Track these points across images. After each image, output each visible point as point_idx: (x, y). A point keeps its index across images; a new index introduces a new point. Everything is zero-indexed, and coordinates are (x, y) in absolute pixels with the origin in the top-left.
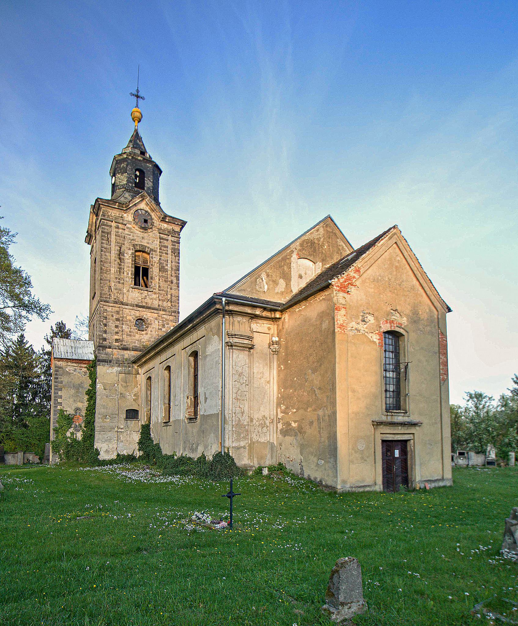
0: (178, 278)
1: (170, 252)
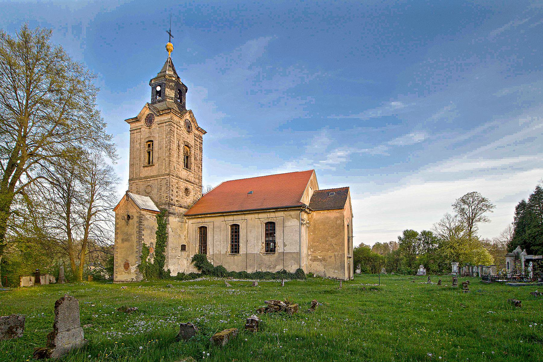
0: (201, 165)
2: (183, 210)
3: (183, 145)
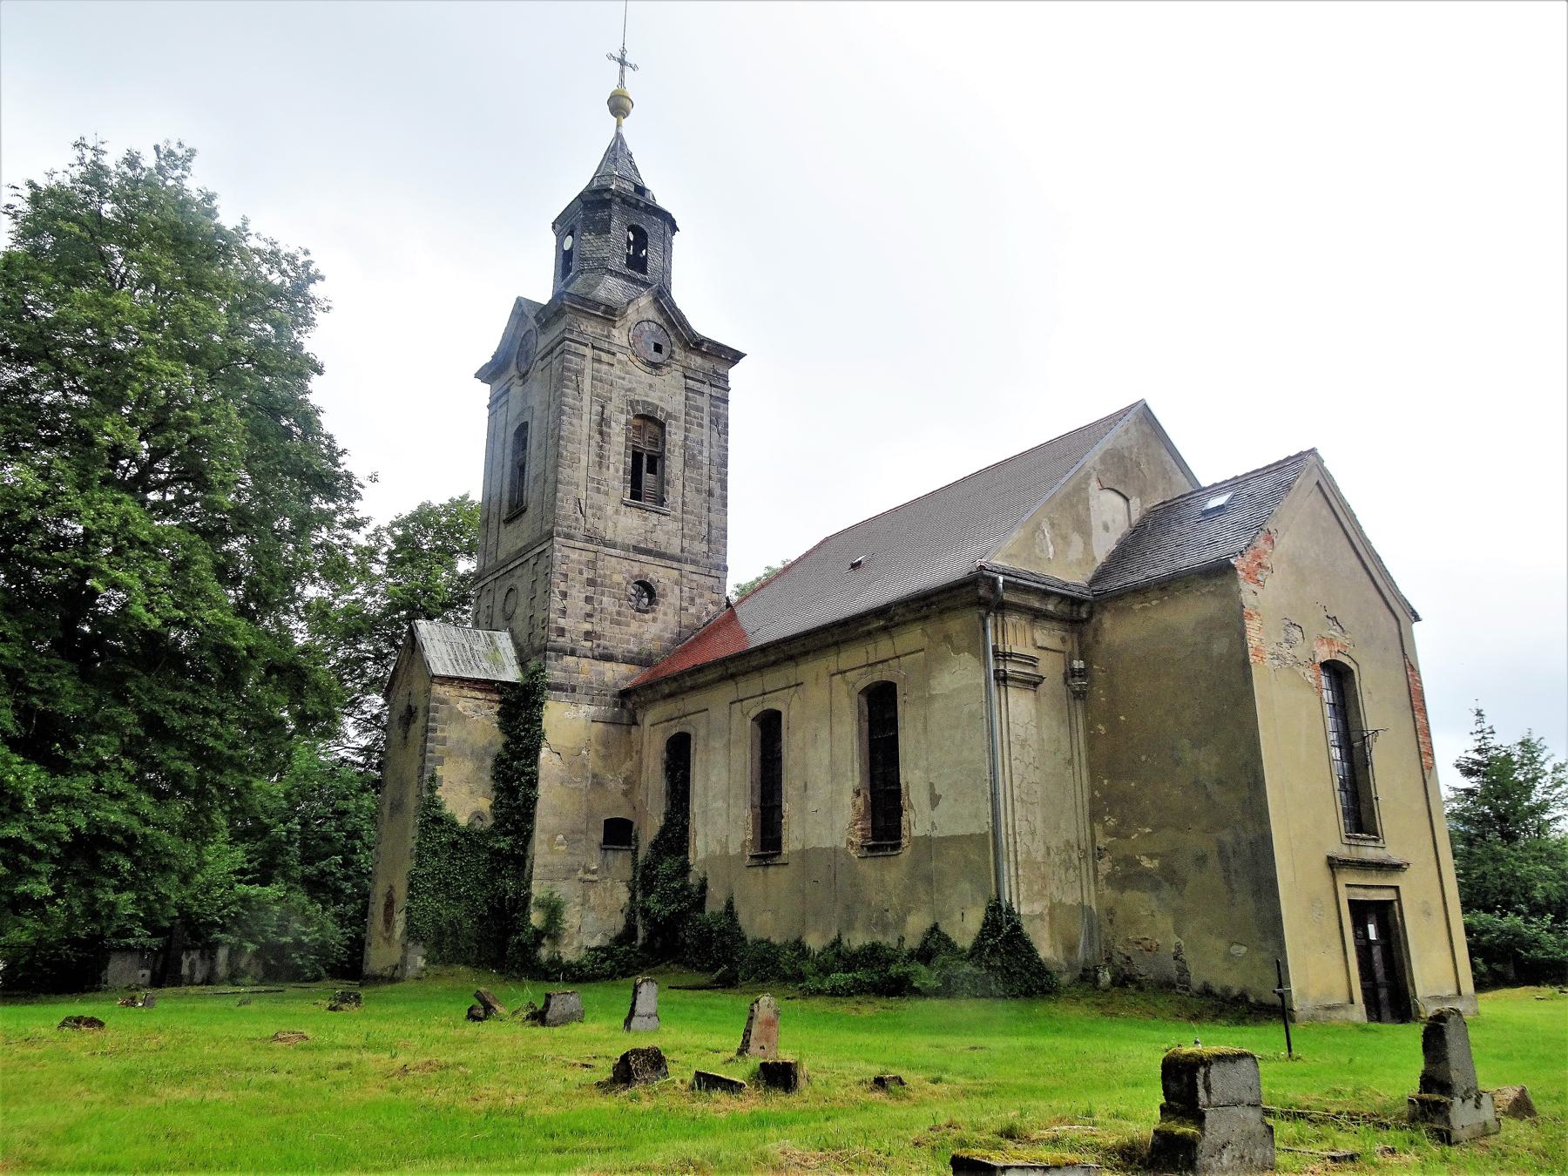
1: (706, 421)
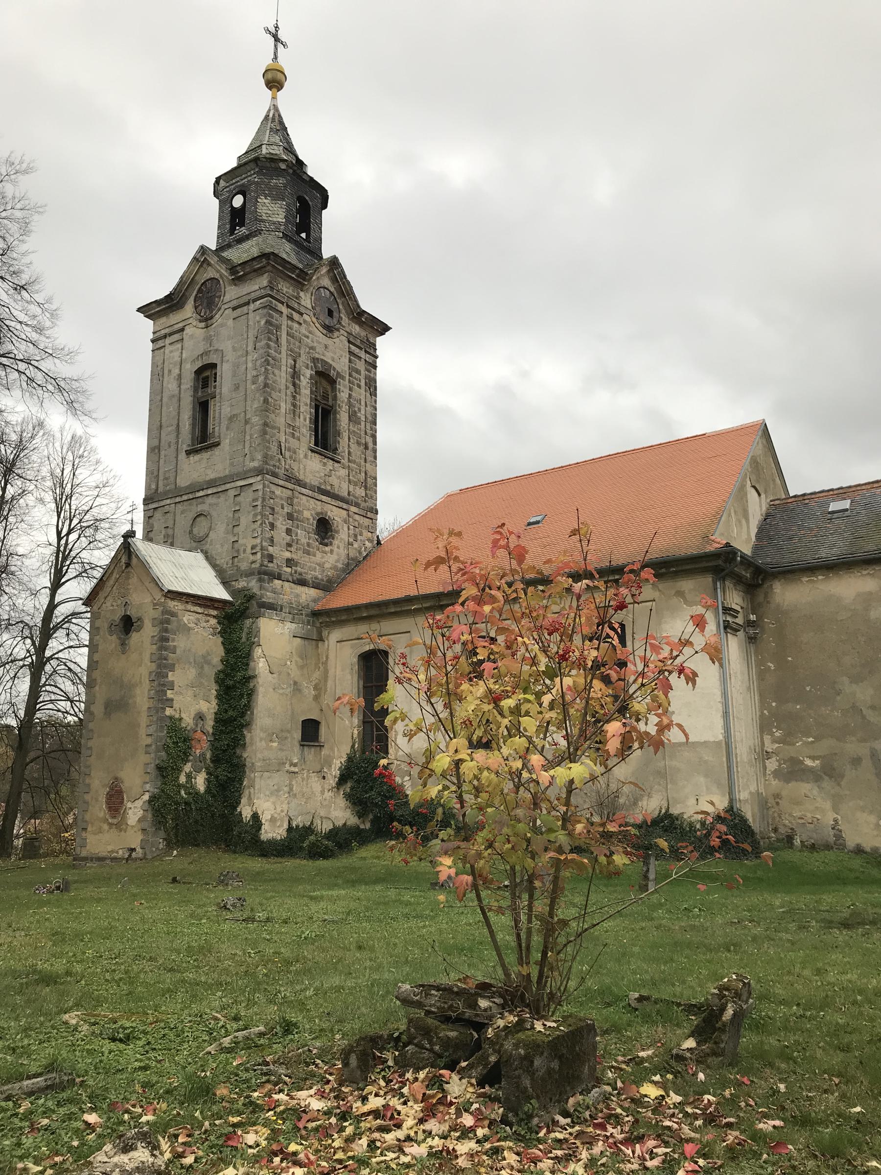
2: (307, 594)
3: (308, 373)
